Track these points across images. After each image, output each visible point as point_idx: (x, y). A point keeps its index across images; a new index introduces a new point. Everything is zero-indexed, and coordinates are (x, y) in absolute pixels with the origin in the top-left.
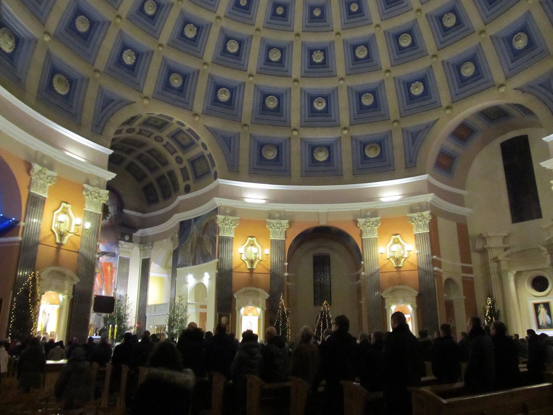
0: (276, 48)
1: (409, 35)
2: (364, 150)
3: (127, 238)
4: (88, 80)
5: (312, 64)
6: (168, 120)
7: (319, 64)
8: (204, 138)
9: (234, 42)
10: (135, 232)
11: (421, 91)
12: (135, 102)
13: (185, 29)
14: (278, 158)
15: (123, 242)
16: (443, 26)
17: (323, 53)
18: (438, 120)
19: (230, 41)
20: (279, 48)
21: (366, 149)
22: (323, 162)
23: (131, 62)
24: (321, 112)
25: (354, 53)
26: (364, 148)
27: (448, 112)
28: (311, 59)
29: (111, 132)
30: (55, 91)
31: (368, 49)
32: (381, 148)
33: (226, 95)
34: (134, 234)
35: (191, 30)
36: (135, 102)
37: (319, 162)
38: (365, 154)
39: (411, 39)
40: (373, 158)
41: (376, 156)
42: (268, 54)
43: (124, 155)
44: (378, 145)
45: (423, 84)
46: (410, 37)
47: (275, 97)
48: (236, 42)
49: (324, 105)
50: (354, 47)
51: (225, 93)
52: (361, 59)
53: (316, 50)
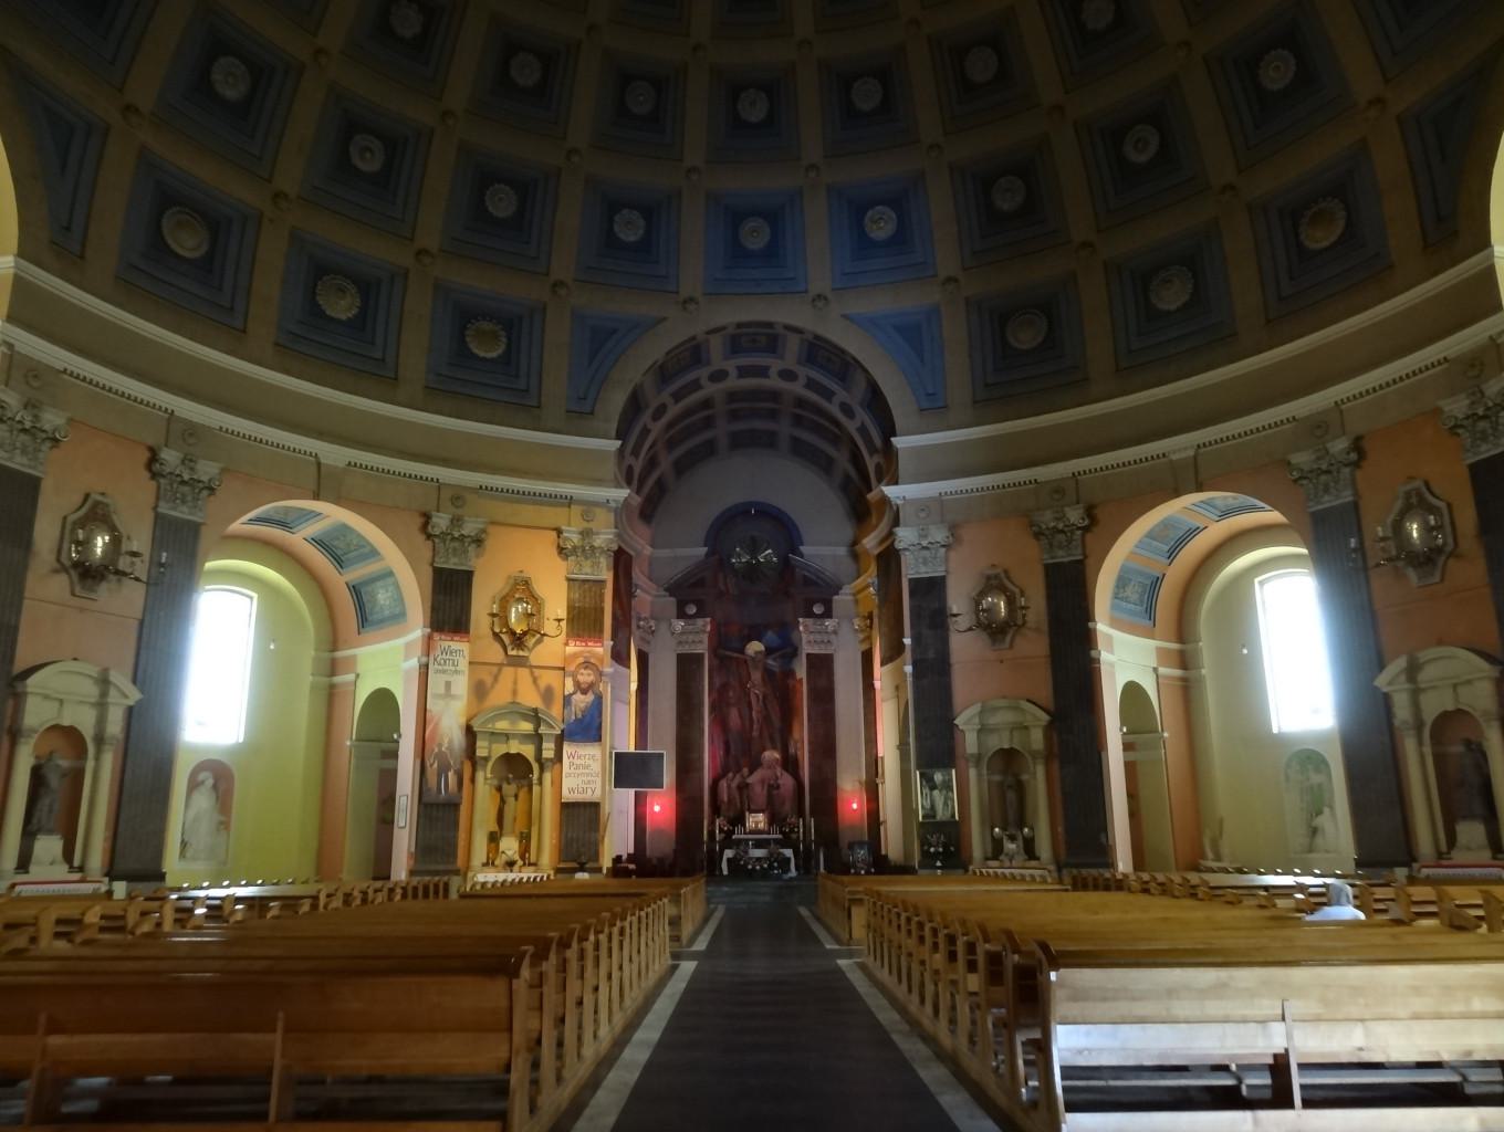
2: (1297, 235)
3: (818, 609)
4: (544, 309)
6: (694, 343)
8: (855, 344)
10: (838, 594)
12: (665, 319)
15: (809, 621)
22: (1178, 310)
29: (615, 401)
30: (476, 357)
34: (836, 597)
36: (665, 319)
37: (1169, 313)
40: (1326, 249)
41: (1333, 238)
43: (708, 435)
51: (881, 218)
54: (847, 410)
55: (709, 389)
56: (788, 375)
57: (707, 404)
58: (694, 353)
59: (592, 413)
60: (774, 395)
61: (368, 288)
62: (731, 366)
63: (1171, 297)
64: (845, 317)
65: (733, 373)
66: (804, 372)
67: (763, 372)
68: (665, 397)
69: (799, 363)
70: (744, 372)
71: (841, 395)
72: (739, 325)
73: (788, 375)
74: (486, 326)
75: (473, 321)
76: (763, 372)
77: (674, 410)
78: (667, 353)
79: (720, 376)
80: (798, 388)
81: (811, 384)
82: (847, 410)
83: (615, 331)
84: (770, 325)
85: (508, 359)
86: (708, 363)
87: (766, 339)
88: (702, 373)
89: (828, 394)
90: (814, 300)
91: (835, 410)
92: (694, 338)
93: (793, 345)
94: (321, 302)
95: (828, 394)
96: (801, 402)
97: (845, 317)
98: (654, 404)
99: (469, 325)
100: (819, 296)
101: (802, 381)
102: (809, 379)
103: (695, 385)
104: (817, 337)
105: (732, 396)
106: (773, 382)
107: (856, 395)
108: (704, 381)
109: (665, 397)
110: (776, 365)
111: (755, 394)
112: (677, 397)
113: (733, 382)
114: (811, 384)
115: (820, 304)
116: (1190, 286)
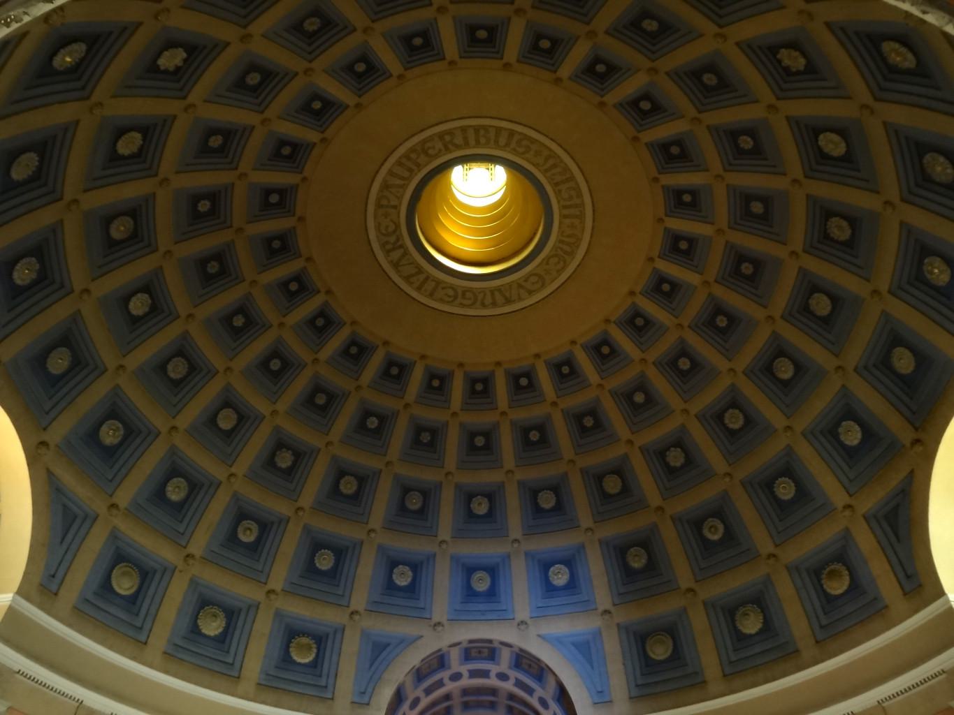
0: (609, 473)
1: (783, 359)
2: (821, 586)
4: (344, 630)
5: (671, 471)
6: (439, 654)
7: (682, 467)
9: (546, 493)
11: (859, 435)
12: (422, 636)
13: (472, 506)
14: (676, 656)
16: (820, 318)
17: (679, 450)
18: (912, 472)
19: (540, 494)
20: (613, 472)
21: (823, 582)
23: (406, 581)
24: (721, 541)
25: (724, 425)
26: (819, 580)
27: (918, 448)
28: (667, 465)
30: (294, 662)
31: (741, 410)
32: (848, 569)
33: (562, 575)
35: (480, 504)
36: (422, 636)
37: (751, 636)
38: (824, 591)
39: (790, 362)
41: (845, 588)
42: (601, 486)
44: (840, 564)
45: (855, 421)
46: (787, 360)
47: (639, 549)
48: (548, 491)
49: (721, 527)
50: (719, 417)
52: (741, 429)
53: (668, 449)
54: (543, 702)
55: (450, 686)
56: (502, 677)
57: (447, 697)
58: (440, 661)
59: (368, 704)
60: (493, 691)
61: (231, 615)
62: (464, 669)
63: (751, 625)
64: (539, 636)
65: (466, 674)
66: (513, 674)
67: (485, 674)
68: (419, 692)
69: (510, 668)
70: (474, 674)
71: (539, 692)
72: (471, 641)
73: (502, 677)
74: (305, 640)
75: (296, 637)
76: (485, 674)
77: (425, 702)
78: (422, 660)
79: (456, 677)
80: (509, 686)
81: (519, 684)
82: (543, 702)
83: (388, 645)
84: (490, 641)
85: (315, 664)
86: (449, 668)
87: (488, 651)
88: (445, 675)
89: (530, 691)
90: (519, 625)
91: (534, 702)
92: (440, 650)
93: (505, 655)
94: (200, 624)
95: (530, 691)
96: (512, 697)
97: (539, 636)
98: (411, 697)
99: (293, 640)
100: (522, 622)
101: (512, 681)
102: (517, 679)
103: (440, 684)
104: (521, 650)
105: (465, 692)
106: (493, 682)
107: (549, 692)
108: (446, 681)
109: (419, 692)
110: (494, 669)
111: (479, 691)
112: (428, 691)
113: (466, 682)
114: (519, 684)
115: (523, 627)
116: (761, 617)
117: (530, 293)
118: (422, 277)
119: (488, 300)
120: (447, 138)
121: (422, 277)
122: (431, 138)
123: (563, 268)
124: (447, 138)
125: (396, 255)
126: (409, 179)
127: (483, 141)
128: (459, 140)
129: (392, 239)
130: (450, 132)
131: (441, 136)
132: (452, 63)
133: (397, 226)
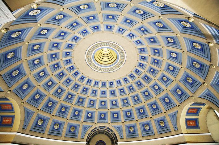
111: (101, 131)
117: (114, 70)
118: (95, 66)
119: (106, 70)
120: (101, 44)
121: (95, 66)
122: (98, 44)
123: (120, 66)
124: (101, 44)
125: (90, 63)
126: (93, 50)
127: (107, 45)
128: (103, 44)
129: (90, 60)
130: (101, 43)
131: (100, 44)
132: (103, 32)
133: (91, 58)
